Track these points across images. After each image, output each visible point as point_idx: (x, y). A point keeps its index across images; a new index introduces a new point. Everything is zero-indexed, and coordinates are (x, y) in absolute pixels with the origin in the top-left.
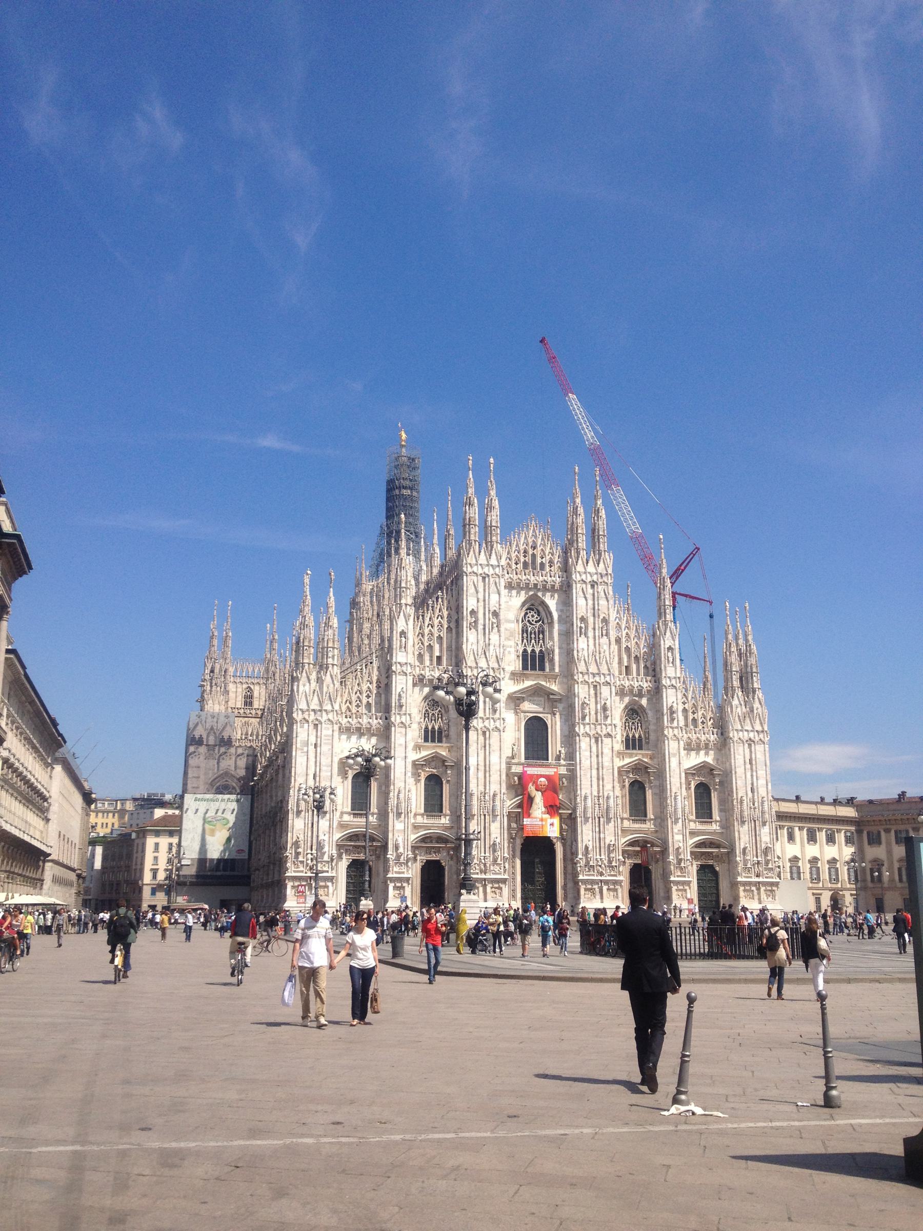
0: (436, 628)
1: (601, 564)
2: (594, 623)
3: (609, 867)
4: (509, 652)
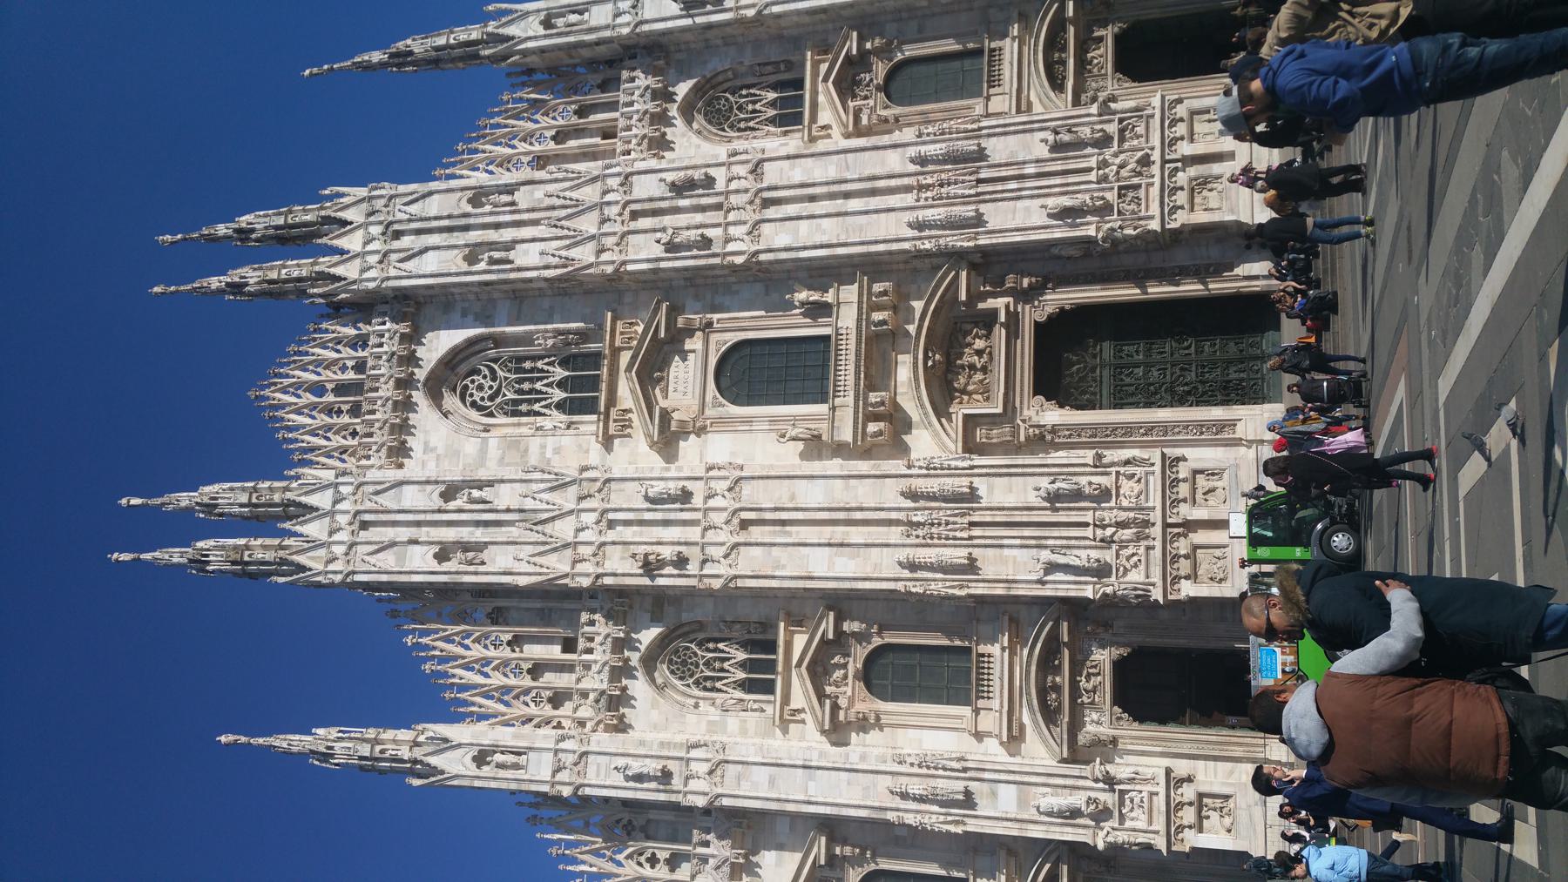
0: (492, 653)
1: (347, 215)
2: (485, 226)
3: (1122, 140)
4: (557, 451)
